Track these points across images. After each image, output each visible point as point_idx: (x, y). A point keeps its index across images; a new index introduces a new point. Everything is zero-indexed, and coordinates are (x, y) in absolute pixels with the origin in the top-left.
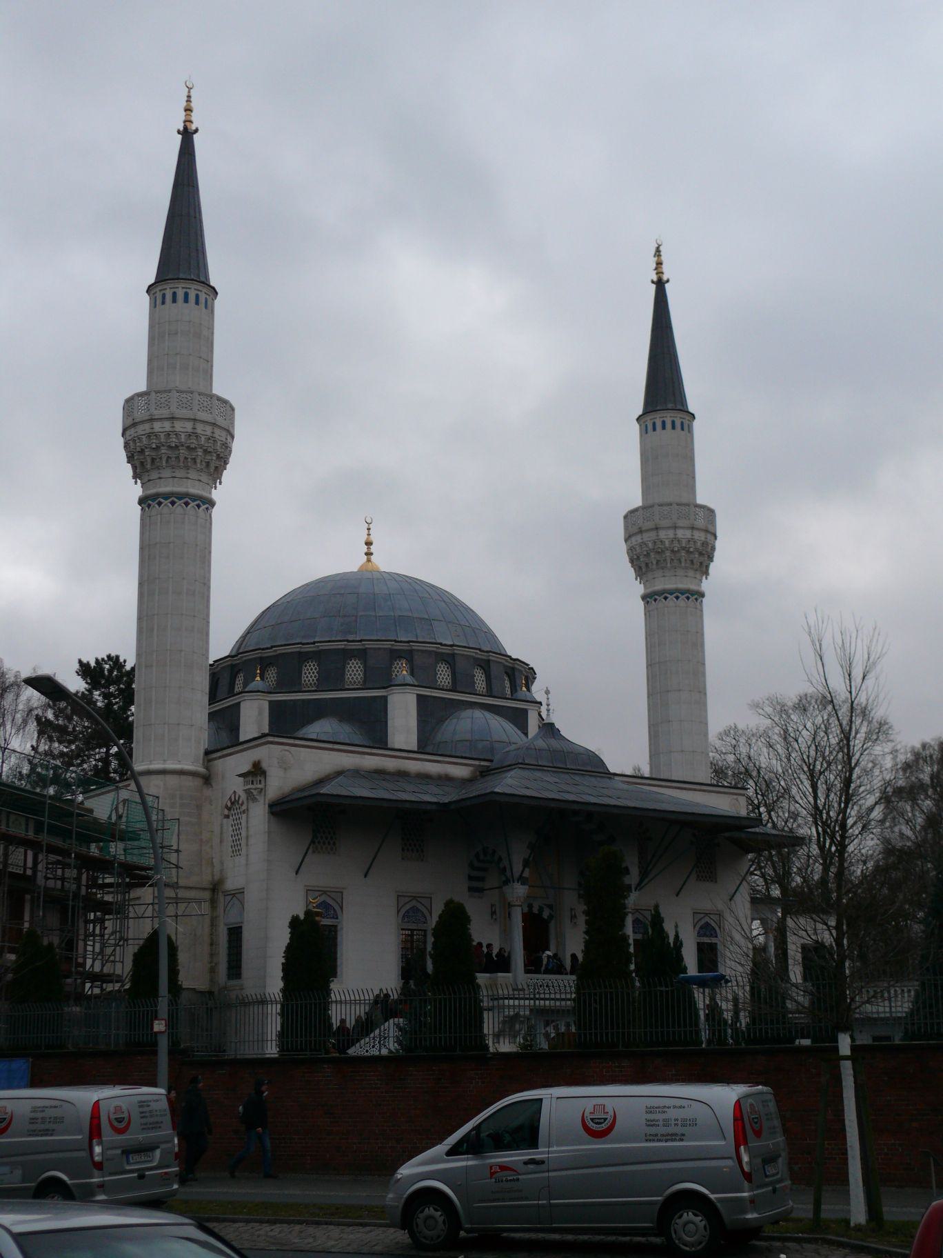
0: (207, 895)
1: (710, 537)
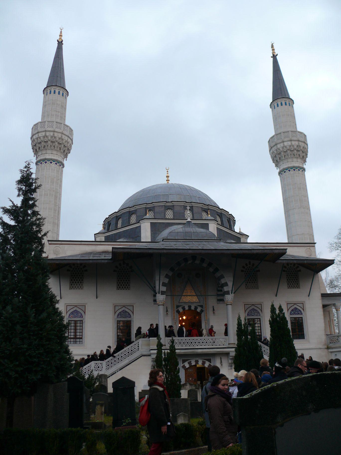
1: (305, 146)
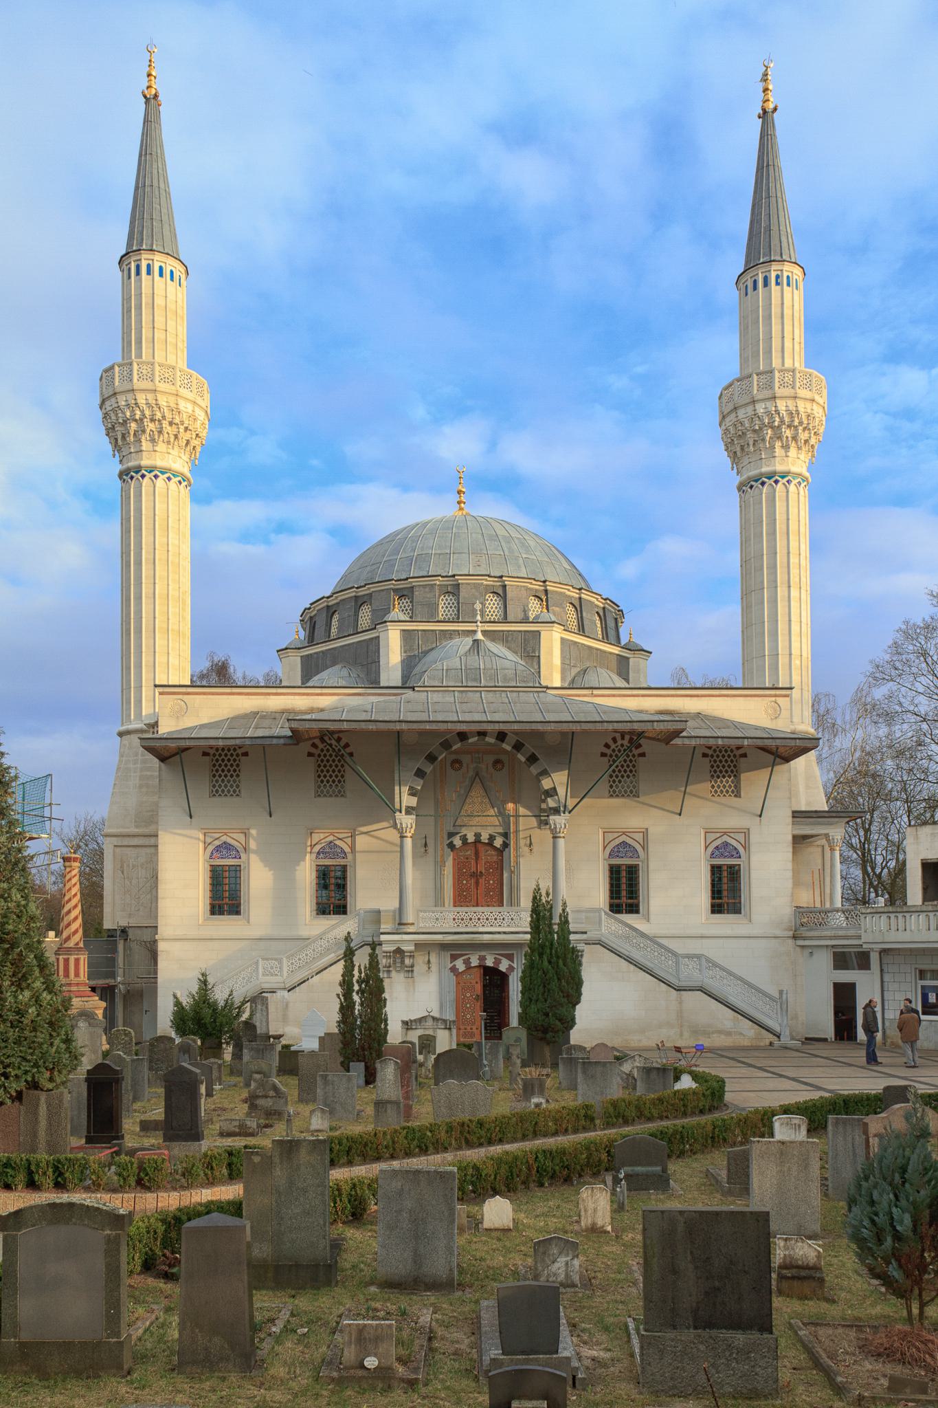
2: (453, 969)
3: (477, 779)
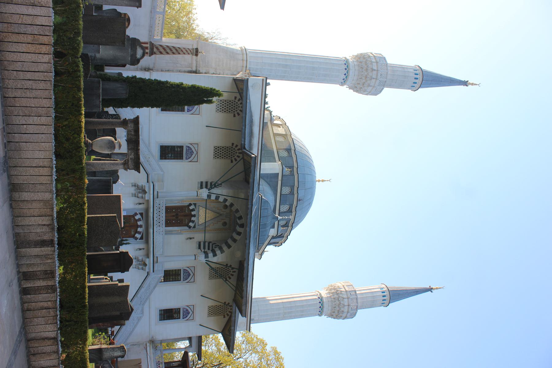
0: (194, 69)
2: (136, 214)
3: (218, 215)
